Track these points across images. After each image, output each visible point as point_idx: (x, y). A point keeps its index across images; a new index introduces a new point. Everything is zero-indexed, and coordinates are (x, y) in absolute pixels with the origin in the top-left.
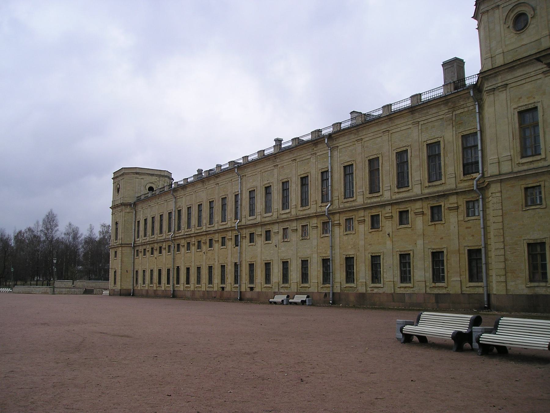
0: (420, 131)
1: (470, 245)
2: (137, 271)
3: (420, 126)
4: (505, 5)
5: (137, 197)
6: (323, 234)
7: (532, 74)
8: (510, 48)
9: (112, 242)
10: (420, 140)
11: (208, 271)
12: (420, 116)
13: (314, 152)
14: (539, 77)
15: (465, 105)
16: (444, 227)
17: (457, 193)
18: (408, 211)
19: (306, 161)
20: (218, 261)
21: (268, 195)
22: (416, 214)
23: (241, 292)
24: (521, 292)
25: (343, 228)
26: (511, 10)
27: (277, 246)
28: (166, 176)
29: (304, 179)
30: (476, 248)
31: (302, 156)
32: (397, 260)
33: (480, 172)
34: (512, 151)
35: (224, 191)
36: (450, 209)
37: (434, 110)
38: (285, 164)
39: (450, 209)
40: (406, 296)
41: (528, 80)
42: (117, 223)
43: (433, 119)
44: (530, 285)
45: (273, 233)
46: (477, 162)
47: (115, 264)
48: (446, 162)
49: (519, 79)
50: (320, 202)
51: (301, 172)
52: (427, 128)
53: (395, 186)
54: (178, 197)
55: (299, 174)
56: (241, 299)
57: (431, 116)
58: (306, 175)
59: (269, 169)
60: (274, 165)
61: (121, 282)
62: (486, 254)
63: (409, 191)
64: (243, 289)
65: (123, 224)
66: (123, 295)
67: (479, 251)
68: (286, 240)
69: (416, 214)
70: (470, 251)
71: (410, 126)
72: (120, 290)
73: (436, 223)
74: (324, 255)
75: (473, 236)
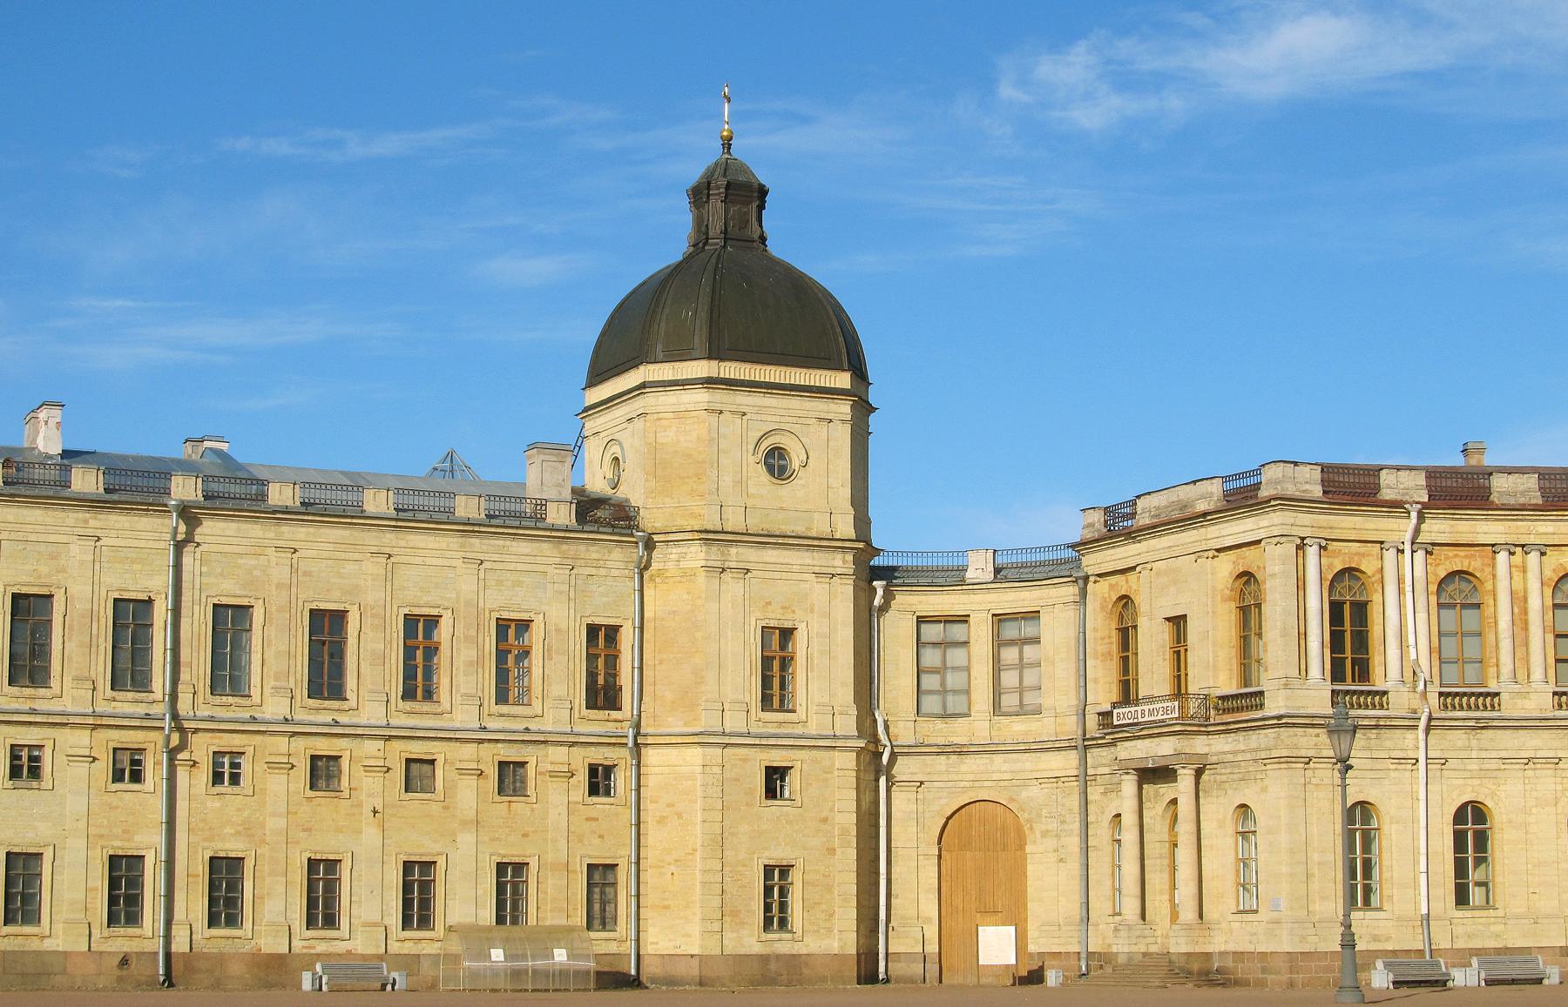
0: (482, 583)
13: (90, 532)
15: (601, 562)
16: (532, 810)
19: (42, 547)
24: (743, 951)
25: (204, 774)
32: (395, 877)
39: (553, 774)
40: (422, 960)
44: (765, 936)
52: (500, 583)
57: (514, 558)
67: (613, 867)
70: (591, 868)
74: (117, 843)
75: (601, 837)
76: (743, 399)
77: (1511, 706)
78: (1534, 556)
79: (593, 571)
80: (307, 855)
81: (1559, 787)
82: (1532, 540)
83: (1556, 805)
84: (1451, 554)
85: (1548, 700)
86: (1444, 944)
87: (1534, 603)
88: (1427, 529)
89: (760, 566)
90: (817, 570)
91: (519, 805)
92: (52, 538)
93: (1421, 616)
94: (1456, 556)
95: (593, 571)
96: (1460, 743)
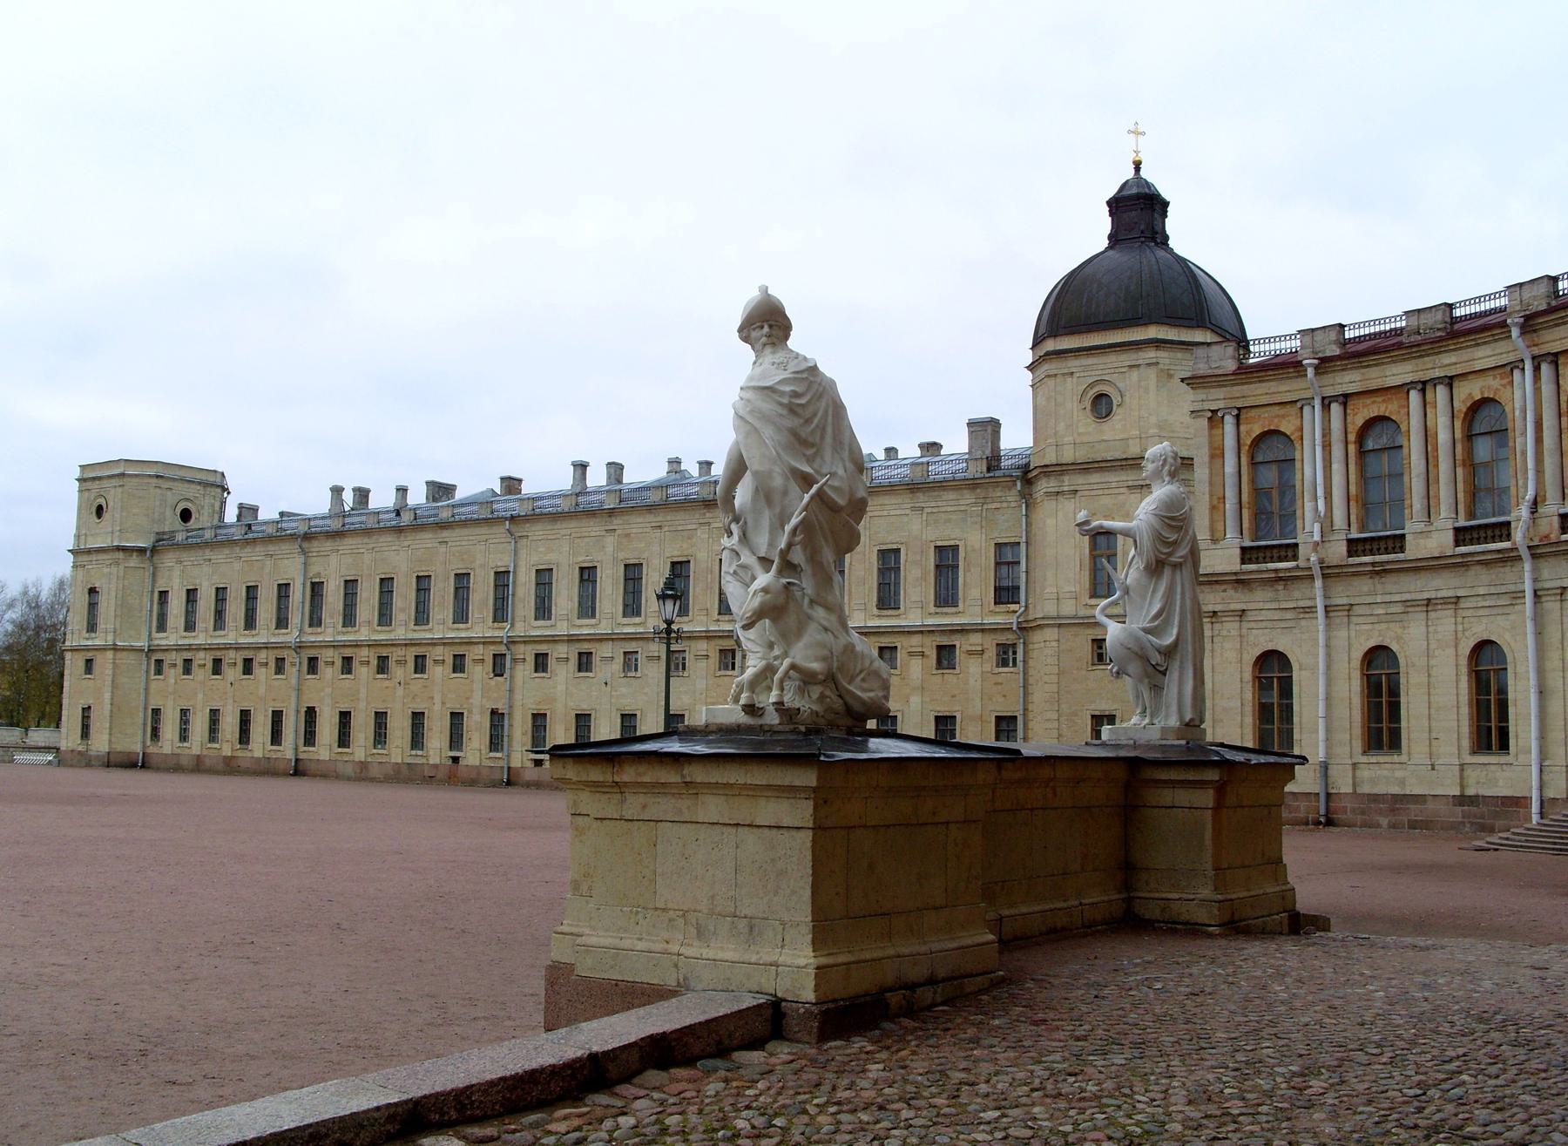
0: (924, 523)
1: (998, 709)
2: (156, 712)
3: (925, 515)
4: (1082, 374)
5: (157, 533)
6: (720, 669)
7: (1114, 485)
8: (1085, 439)
9: (75, 637)
10: (924, 537)
11: (410, 721)
12: (926, 499)
13: (706, 521)
14: (1122, 490)
17: (983, 631)
18: (896, 647)
19: (685, 533)
20: (443, 703)
21: (586, 583)
22: (911, 654)
23: (509, 768)
26: (1091, 386)
27: (609, 683)
28: (213, 485)
29: (679, 566)
30: (1009, 714)
31: (677, 523)
33: (1023, 604)
34: (1078, 585)
35: (463, 560)
36: (970, 653)
37: (951, 495)
38: (634, 531)
39: (970, 653)
41: (1106, 492)
42: (93, 591)
43: (949, 509)
45: (598, 659)
46: (1018, 588)
47: (75, 691)
48: (968, 580)
49: (1095, 487)
50: (717, 612)
51: (675, 552)
52: (936, 521)
53: (874, 604)
54: (314, 554)
55: (668, 555)
56: (509, 783)
57: (944, 504)
58: (685, 559)
59: (593, 534)
60: (607, 528)
61: (110, 734)
62: (1025, 724)
63: (899, 615)
64: (516, 763)
65: (119, 596)
66: (116, 766)
68: (633, 674)
69: (911, 654)
70: (998, 719)
71: (908, 512)
72: (109, 753)
73: (945, 671)
75: (1005, 696)
76: (1073, 364)
77: (1417, 548)
78: (1441, 391)
79: (998, 505)
80: (374, 710)
81: (1460, 628)
82: (1438, 373)
83: (1456, 647)
84: (1368, 401)
85: (1450, 536)
86: (1346, 788)
87: (1443, 437)
88: (1340, 381)
89: (1086, 487)
90: (1130, 483)
91: (950, 677)
92: (689, 527)
93: (1337, 467)
94: (1374, 402)
95: (998, 505)
96: (1365, 589)
